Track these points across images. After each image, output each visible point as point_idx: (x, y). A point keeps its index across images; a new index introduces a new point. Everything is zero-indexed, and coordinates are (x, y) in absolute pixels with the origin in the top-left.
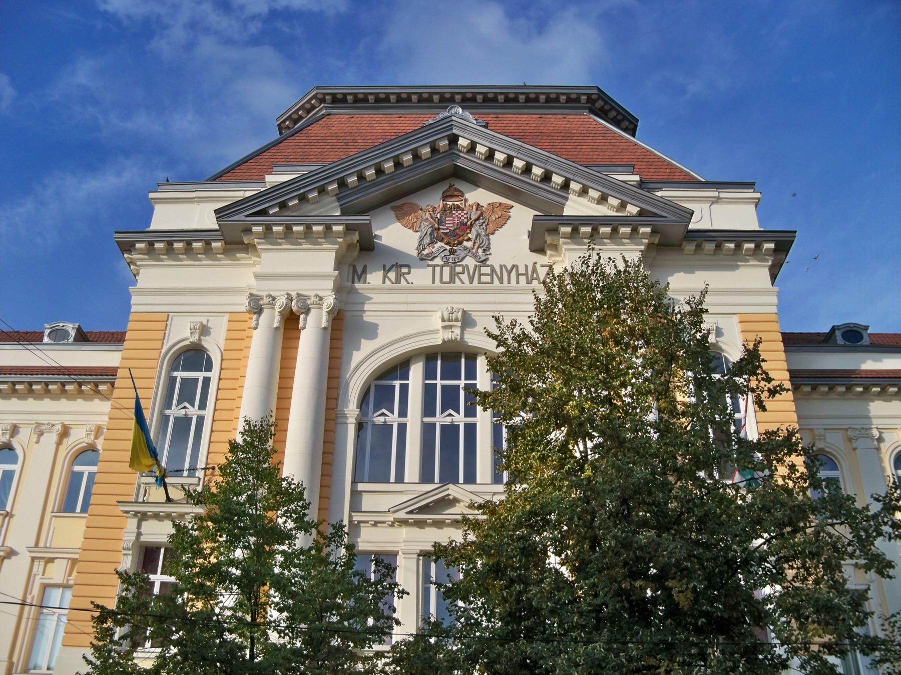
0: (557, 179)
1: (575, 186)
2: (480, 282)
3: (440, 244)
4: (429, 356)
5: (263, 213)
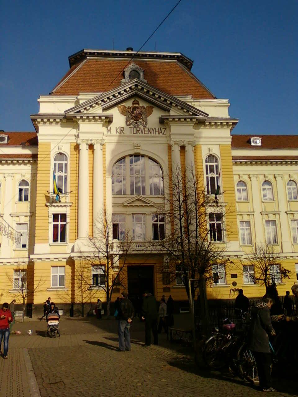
2: (145, 134)
3: (132, 120)
4: (131, 156)
5: (79, 112)
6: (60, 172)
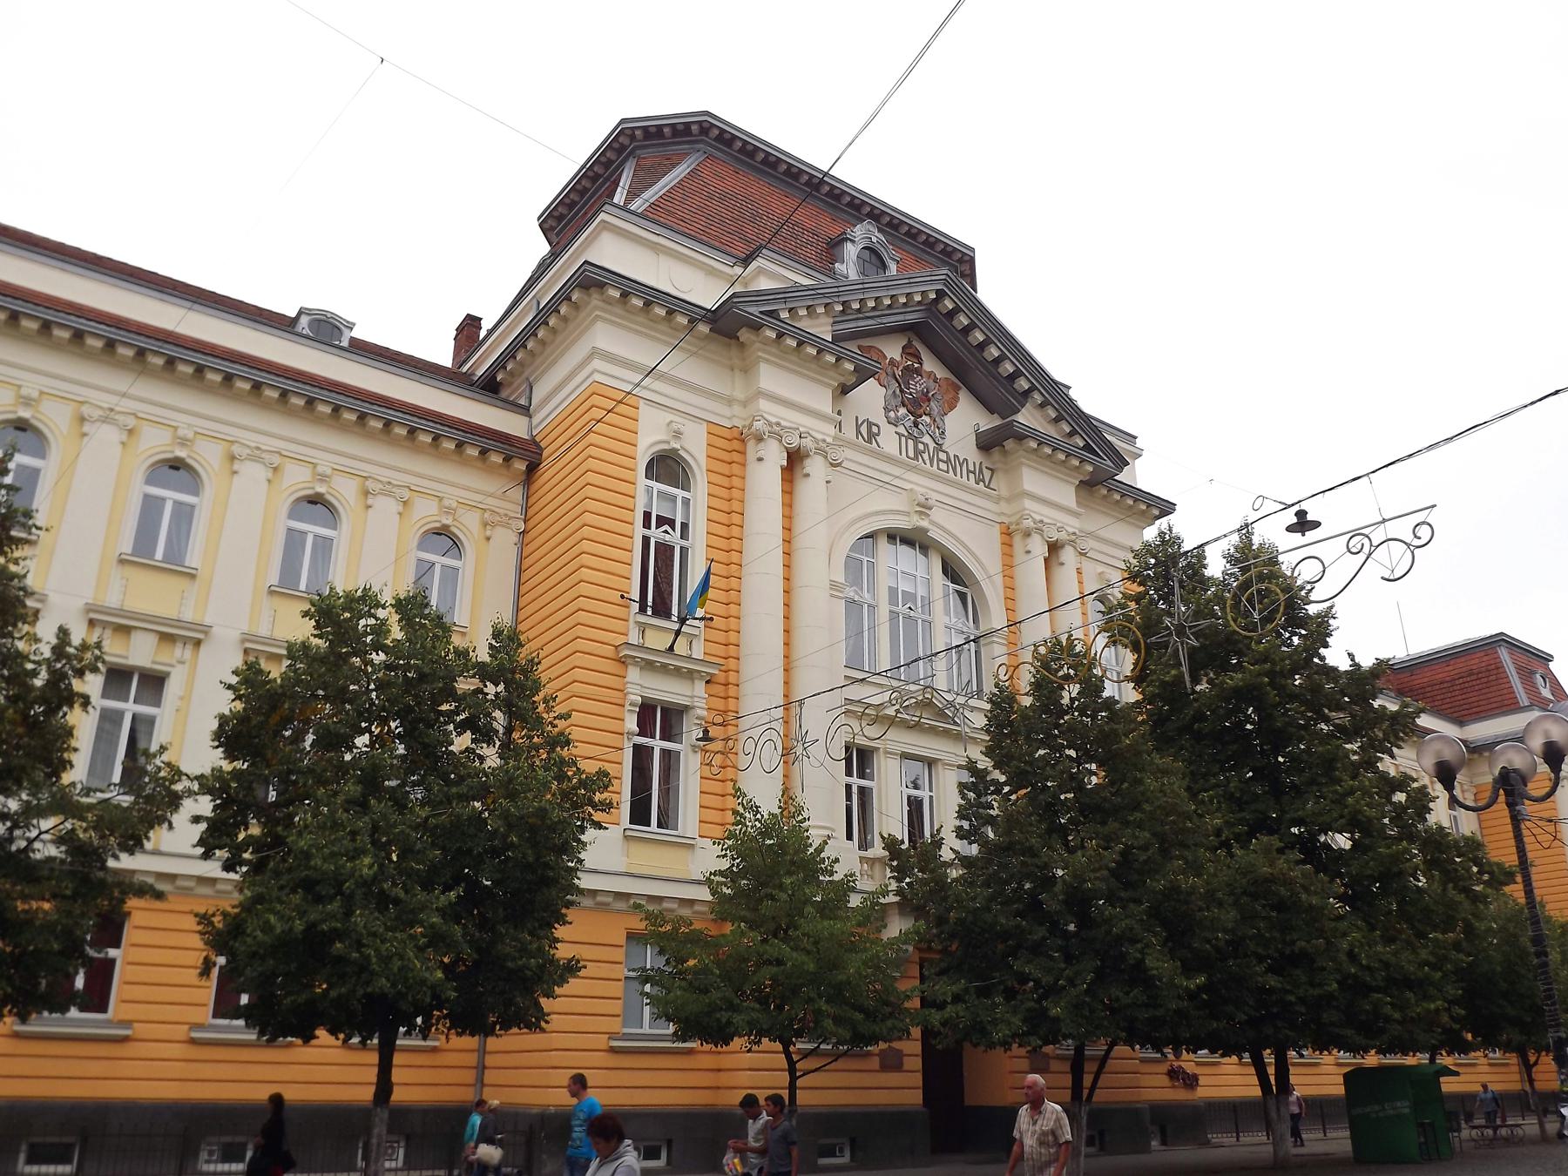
0: (1023, 384)
1: (1036, 396)
6: (666, 527)
